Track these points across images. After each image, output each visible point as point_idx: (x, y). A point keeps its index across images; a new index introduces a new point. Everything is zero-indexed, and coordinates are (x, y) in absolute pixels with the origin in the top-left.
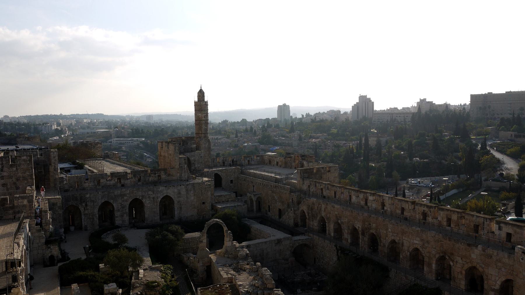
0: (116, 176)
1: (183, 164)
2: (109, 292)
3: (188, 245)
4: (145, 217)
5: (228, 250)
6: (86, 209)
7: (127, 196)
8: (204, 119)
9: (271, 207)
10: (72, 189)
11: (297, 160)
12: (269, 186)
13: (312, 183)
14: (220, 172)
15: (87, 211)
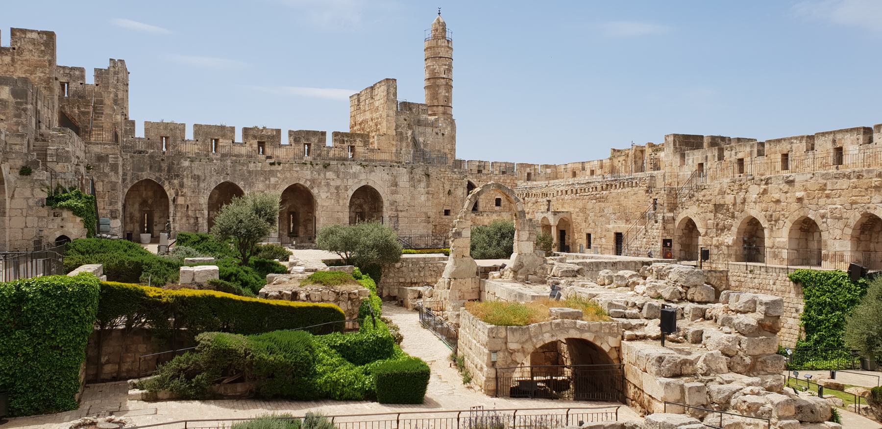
0: (255, 137)
1: (404, 127)
2: (193, 280)
3: (417, 274)
4: (317, 229)
5: (525, 264)
6: (180, 193)
7: (277, 177)
8: (444, 76)
9: (592, 236)
10: (152, 151)
11: (640, 159)
12: (591, 190)
13: (709, 155)
14: (475, 180)
15: (183, 198)
